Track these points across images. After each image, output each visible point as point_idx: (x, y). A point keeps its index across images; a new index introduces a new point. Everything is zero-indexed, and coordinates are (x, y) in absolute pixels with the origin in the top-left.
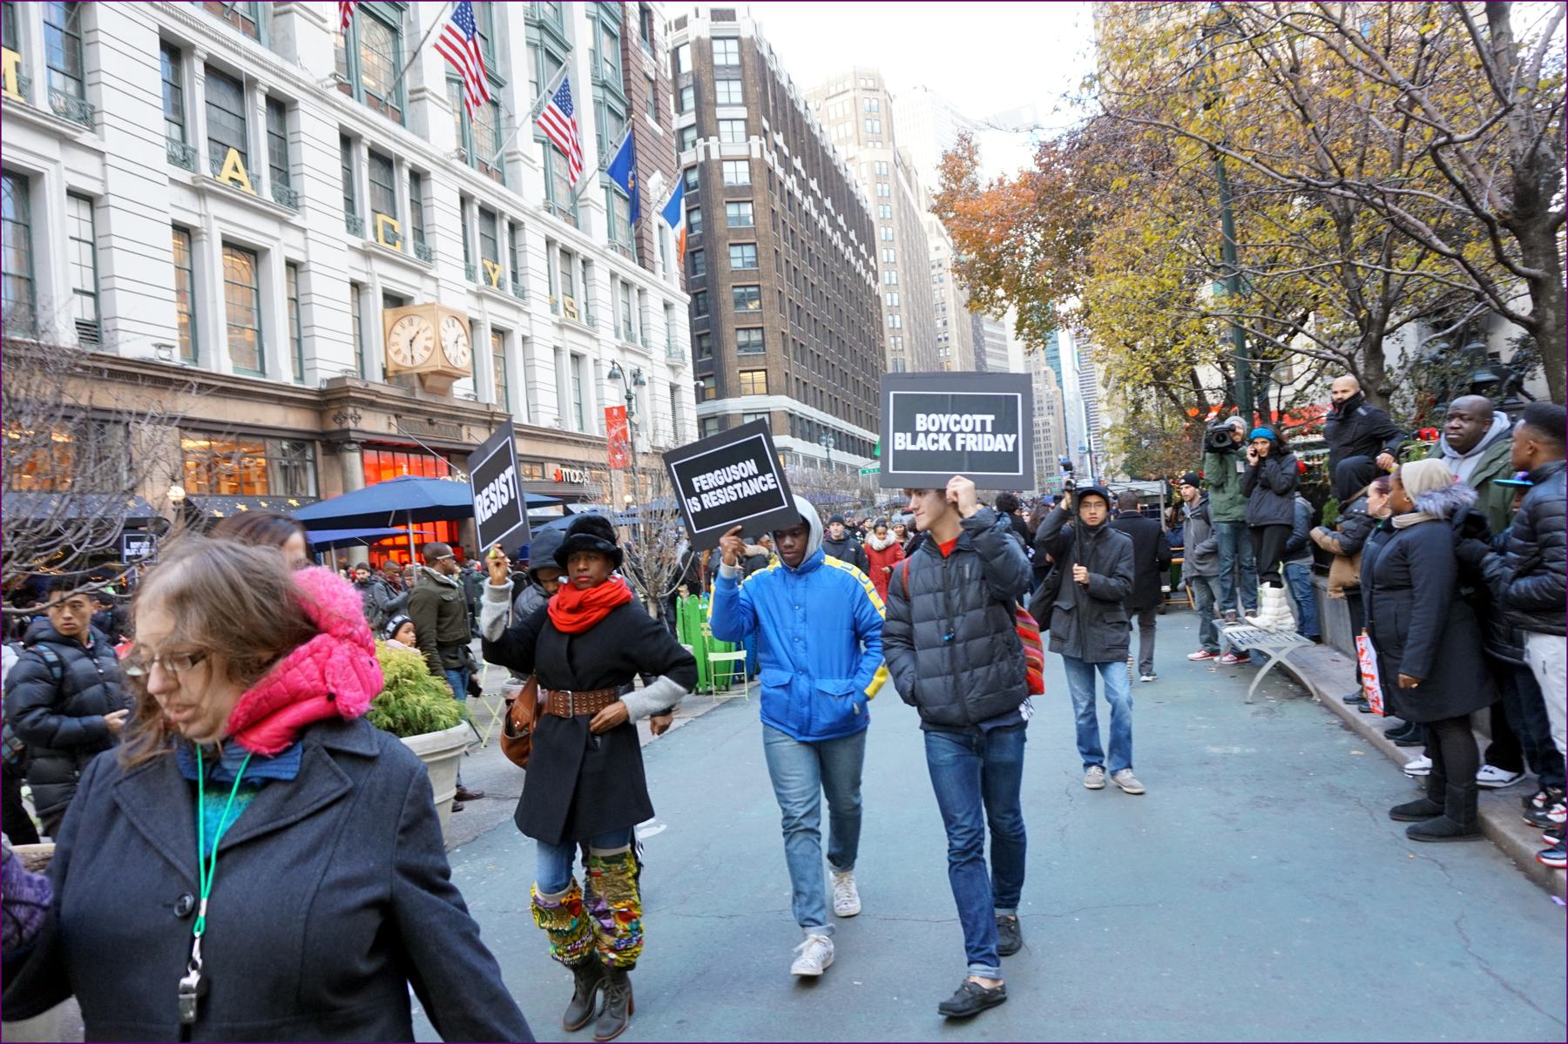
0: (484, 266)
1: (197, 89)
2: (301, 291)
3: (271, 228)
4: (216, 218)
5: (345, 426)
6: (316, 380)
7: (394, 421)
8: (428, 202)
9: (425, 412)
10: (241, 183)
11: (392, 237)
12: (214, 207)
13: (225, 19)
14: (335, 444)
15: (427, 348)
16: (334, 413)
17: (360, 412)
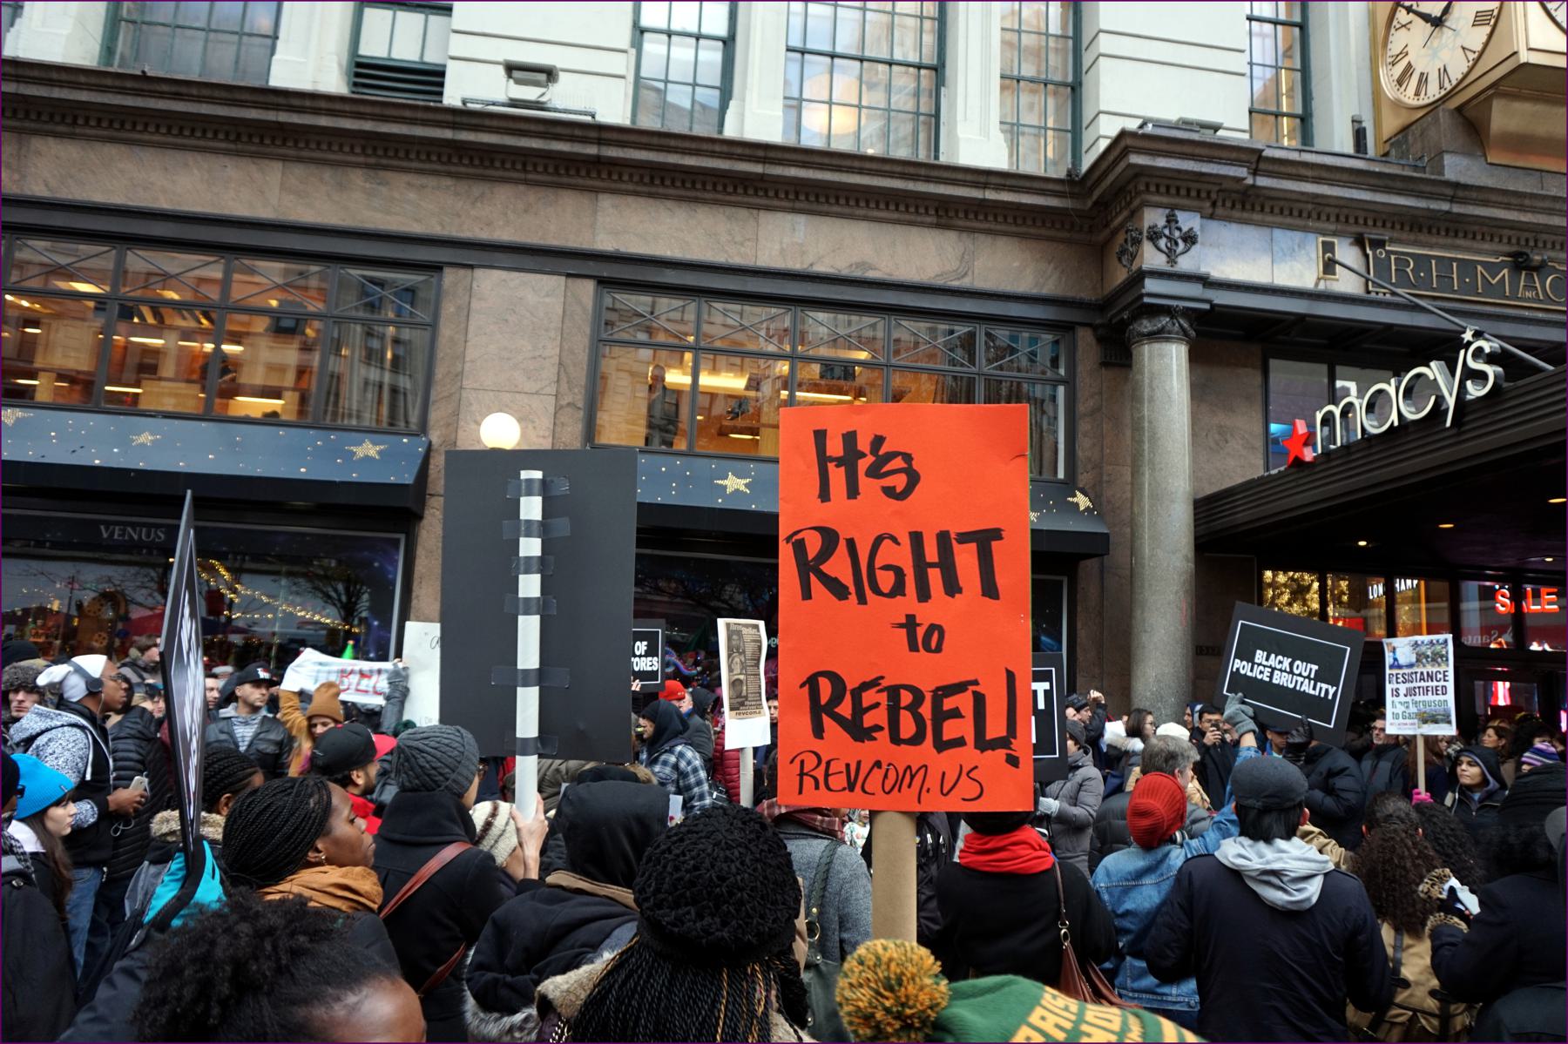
7: (1347, 253)
17: (1189, 221)
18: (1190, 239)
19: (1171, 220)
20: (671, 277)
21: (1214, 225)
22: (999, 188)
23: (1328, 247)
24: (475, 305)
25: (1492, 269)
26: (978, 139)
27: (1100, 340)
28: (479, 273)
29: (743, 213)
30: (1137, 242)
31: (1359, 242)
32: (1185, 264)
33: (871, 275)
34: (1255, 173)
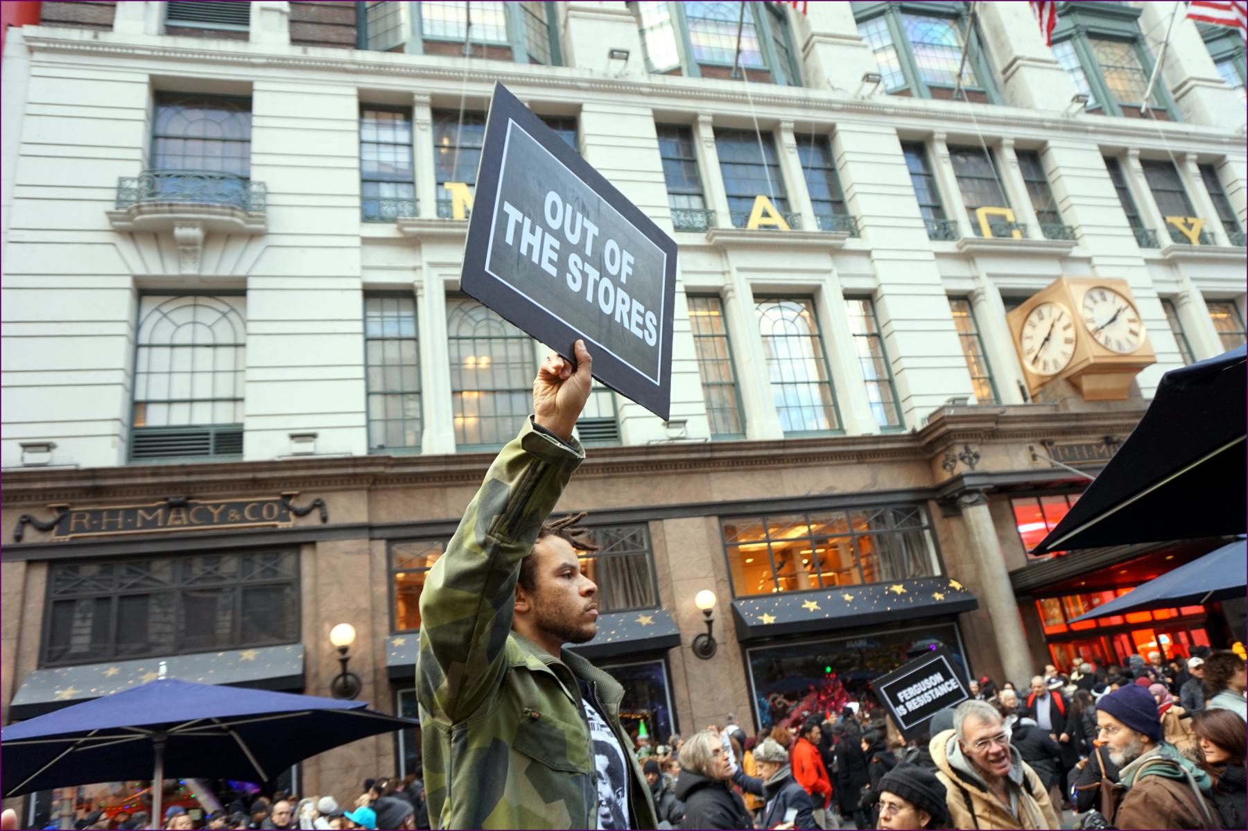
0: (1170, 227)
1: (708, 154)
2: (882, 323)
3: (824, 262)
4: (740, 270)
5: (957, 472)
6: (916, 421)
7: (1040, 451)
8: (1054, 176)
9: (1094, 430)
10: (775, 227)
11: (1002, 228)
12: (736, 260)
13: (735, 79)
14: (950, 500)
15: (1067, 341)
16: (942, 458)
17: (975, 449)
18: (977, 456)
19: (967, 450)
20: (750, 509)
21: (984, 448)
22: (884, 442)
23: (1031, 449)
24: (668, 538)
25: (1099, 446)
26: (864, 417)
27: (940, 505)
28: (666, 522)
29: (774, 472)
30: (954, 461)
31: (1043, 443)
32: (979, 467)
33: (836, 492)
34: (997, 423)
